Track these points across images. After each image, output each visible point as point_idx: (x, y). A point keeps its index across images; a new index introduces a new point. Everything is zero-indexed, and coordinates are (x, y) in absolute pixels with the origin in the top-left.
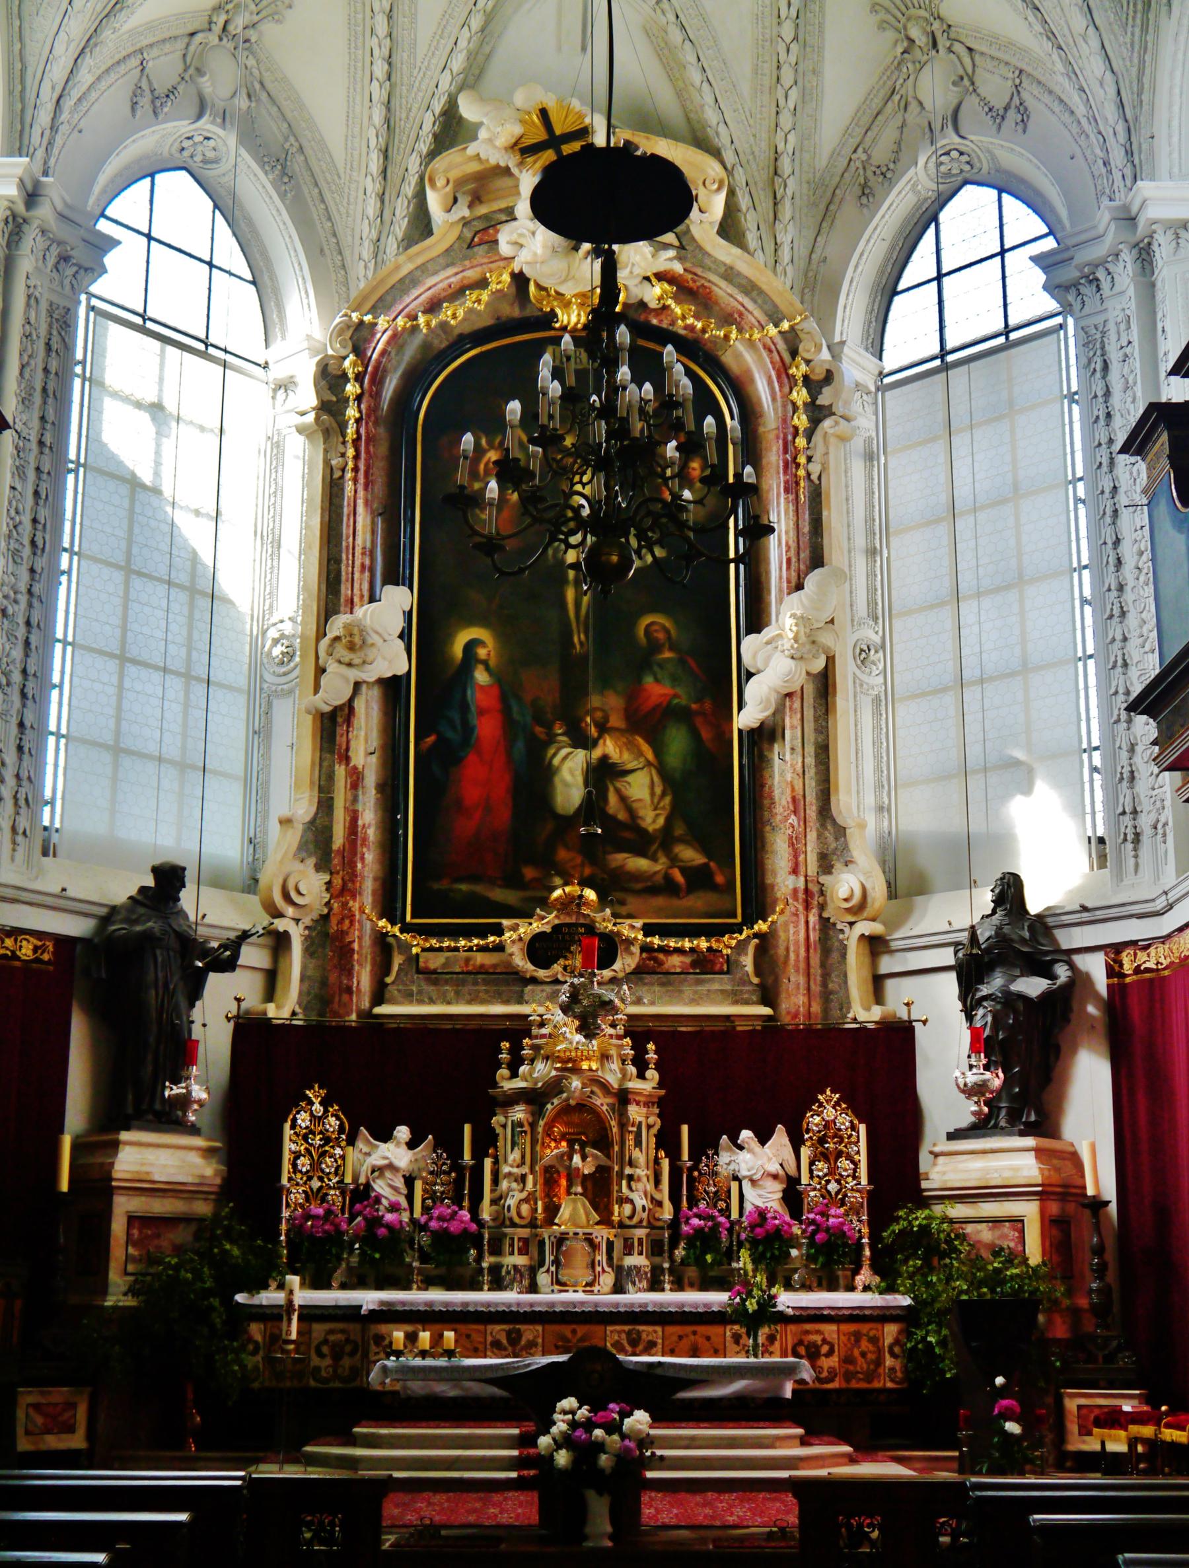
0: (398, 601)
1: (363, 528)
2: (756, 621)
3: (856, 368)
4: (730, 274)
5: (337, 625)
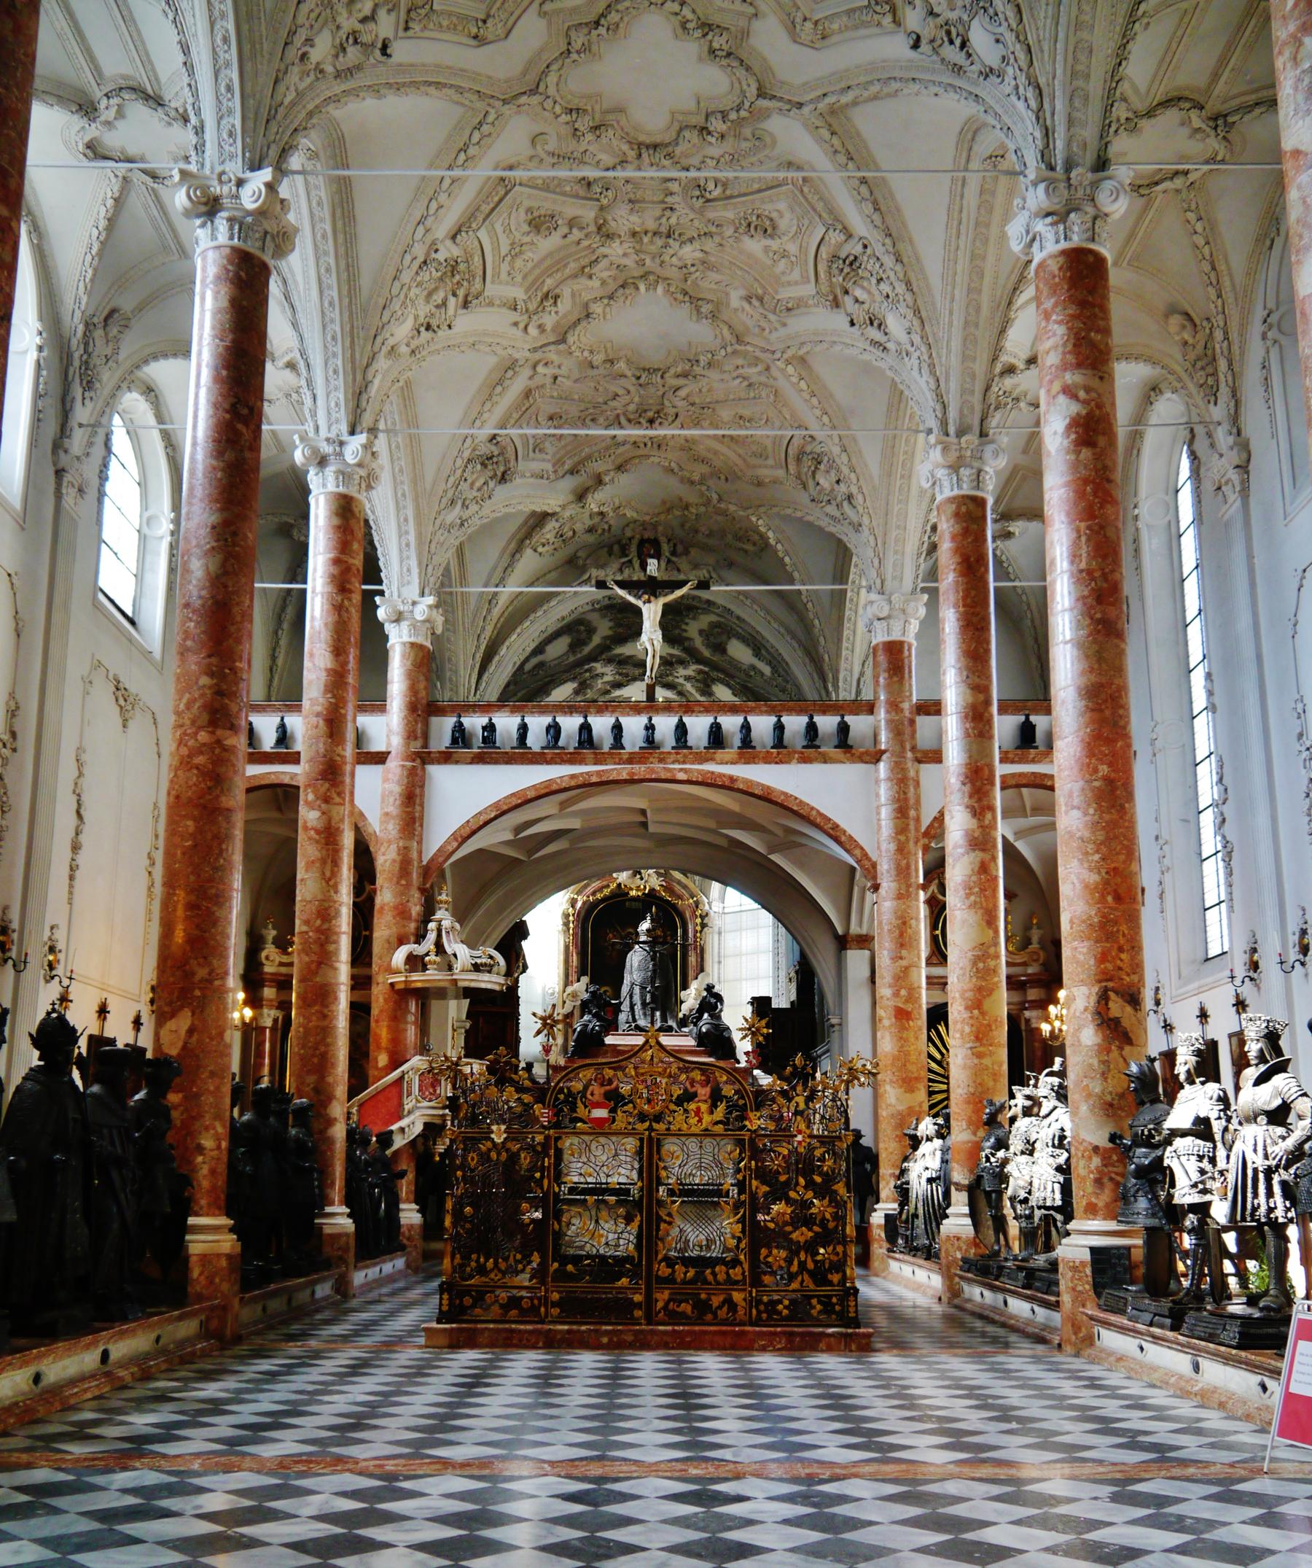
0: (585, 979)
1: (575, 960)
2: (685, 986)
3: (716, 907)
4: (679, 883)
5: (569, 989)
